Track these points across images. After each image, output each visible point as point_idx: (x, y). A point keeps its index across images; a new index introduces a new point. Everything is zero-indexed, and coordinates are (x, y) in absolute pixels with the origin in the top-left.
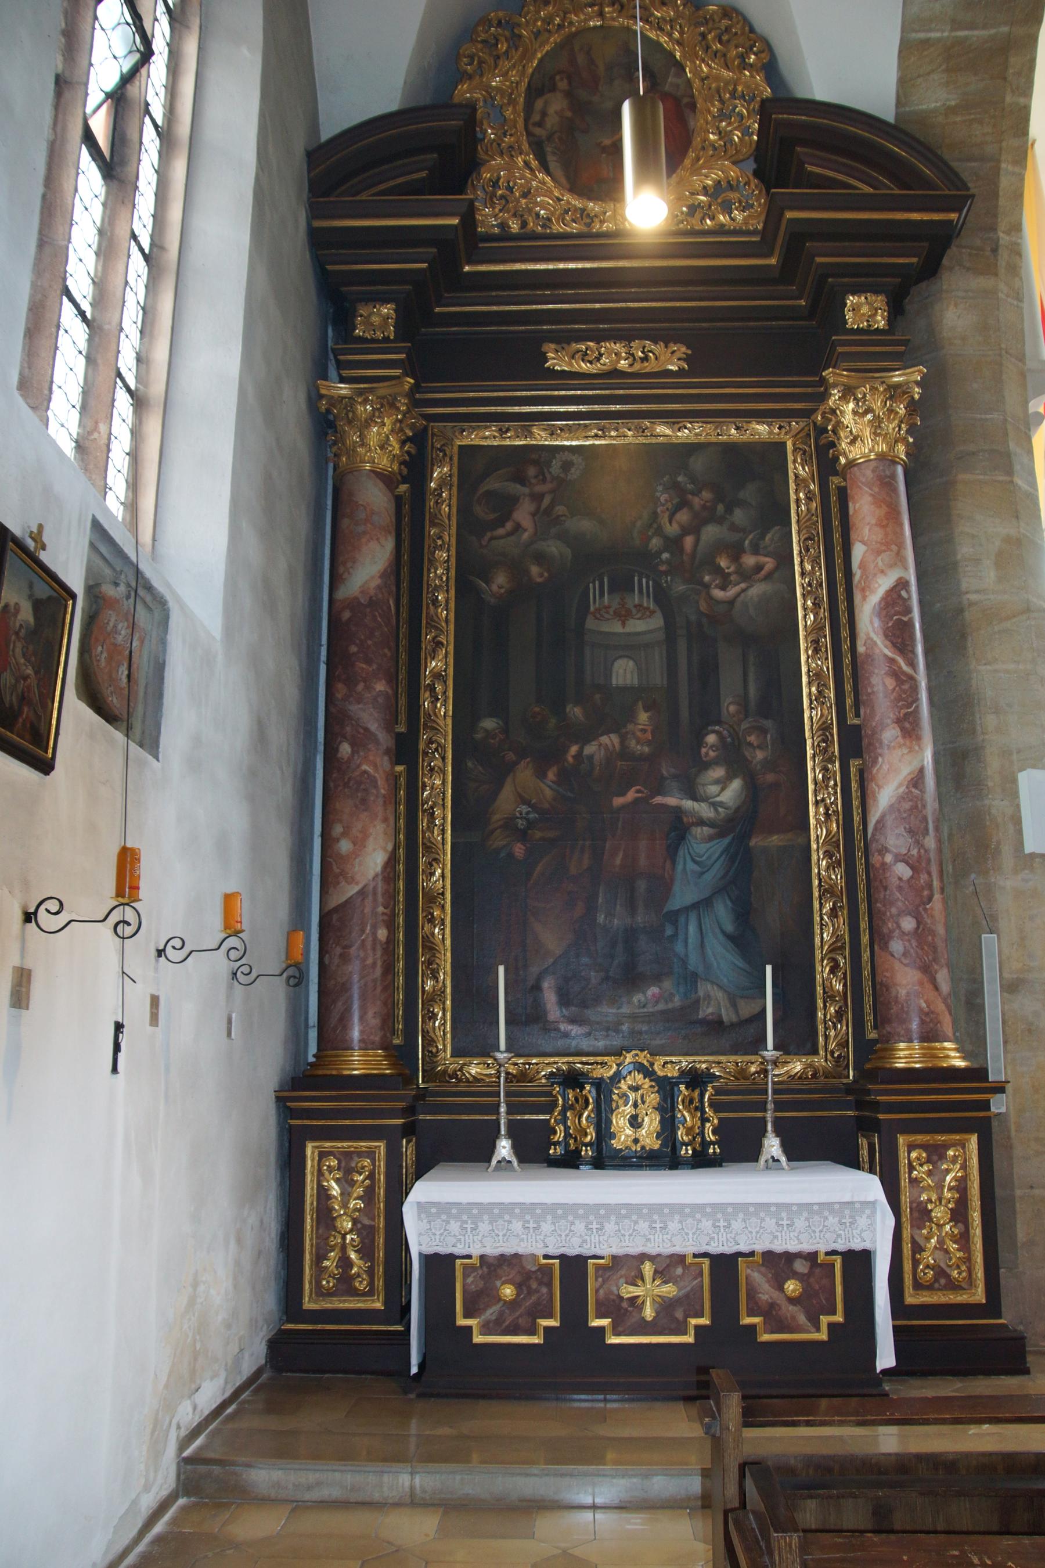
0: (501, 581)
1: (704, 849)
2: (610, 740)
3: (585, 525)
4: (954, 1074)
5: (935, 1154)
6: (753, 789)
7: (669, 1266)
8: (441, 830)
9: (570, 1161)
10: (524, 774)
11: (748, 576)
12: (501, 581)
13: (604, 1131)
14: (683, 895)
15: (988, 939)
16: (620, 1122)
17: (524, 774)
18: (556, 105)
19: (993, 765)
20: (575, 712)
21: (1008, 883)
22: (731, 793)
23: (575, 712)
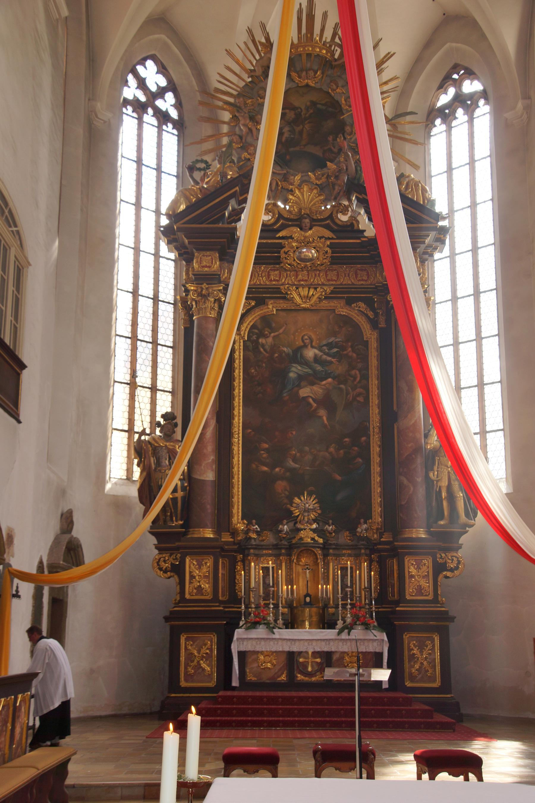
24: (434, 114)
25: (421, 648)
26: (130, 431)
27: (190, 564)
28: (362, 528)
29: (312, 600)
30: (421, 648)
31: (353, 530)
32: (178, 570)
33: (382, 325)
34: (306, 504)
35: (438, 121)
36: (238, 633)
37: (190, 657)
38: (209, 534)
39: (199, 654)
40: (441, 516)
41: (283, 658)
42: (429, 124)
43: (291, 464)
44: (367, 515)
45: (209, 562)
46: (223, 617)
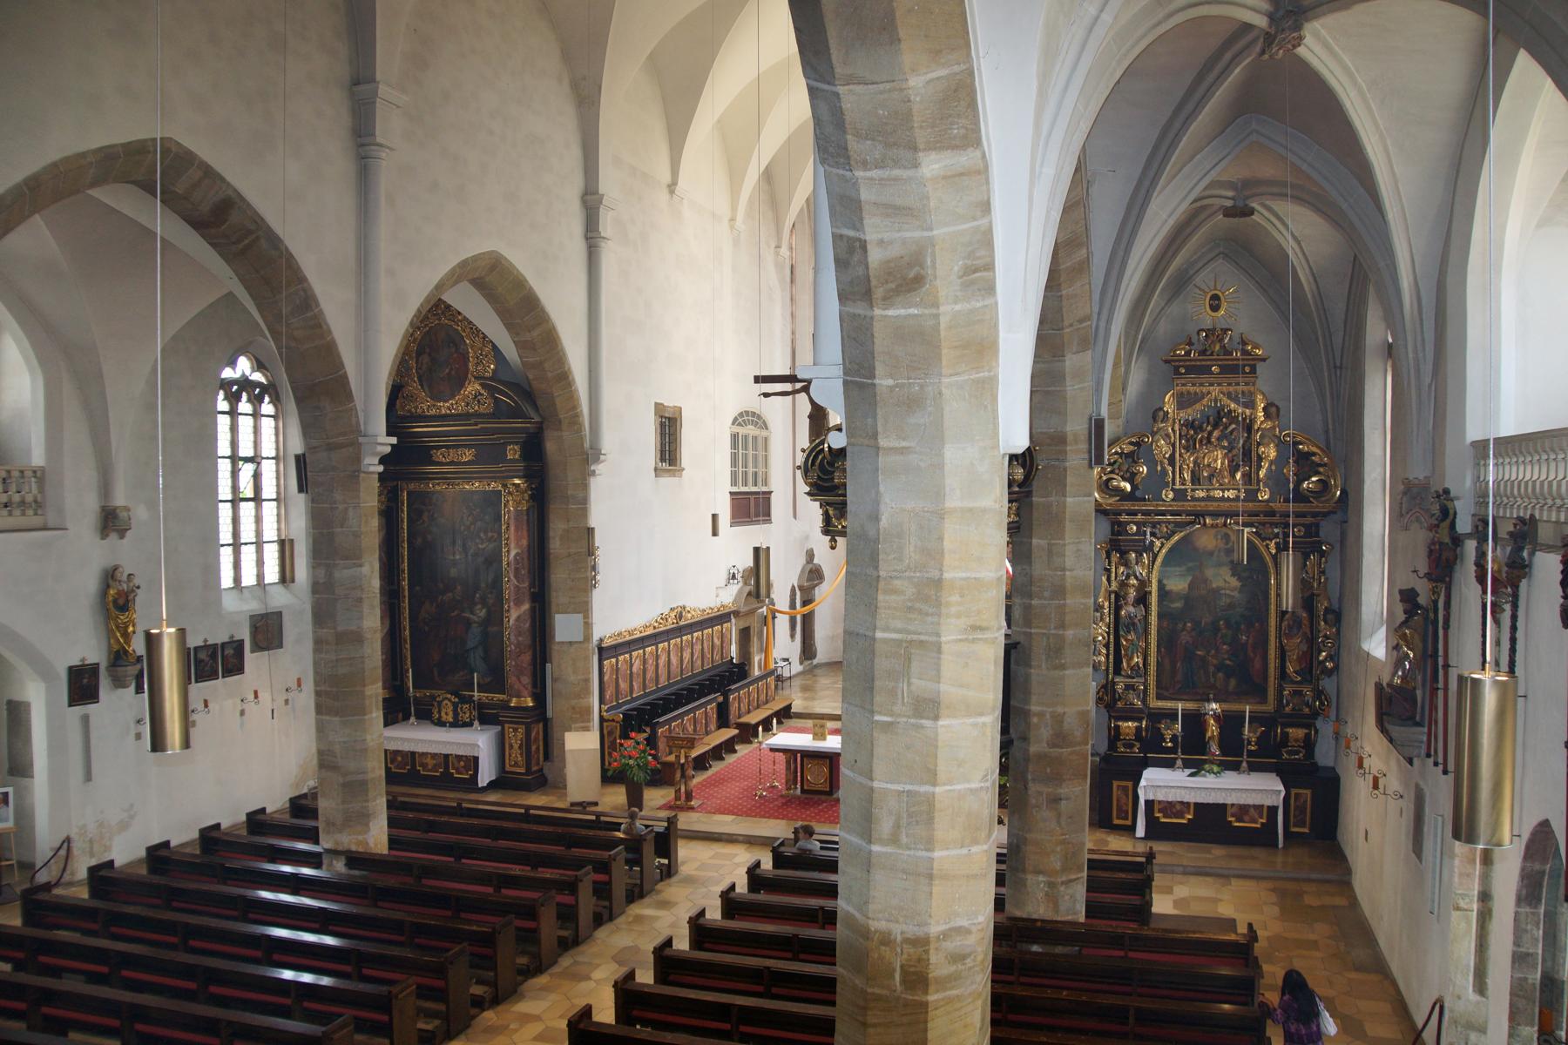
1: (476, 629)
4: (526, 709)
5: (515, 730)
6: (489, 613)
7: (434, 756)
8: (407, 623)
11: (490, 540)
14: (470, 644)
15: (548, 666)
18: (425, 359)
19: (554, 608)
21: (555, 647)
22: (483, 613)
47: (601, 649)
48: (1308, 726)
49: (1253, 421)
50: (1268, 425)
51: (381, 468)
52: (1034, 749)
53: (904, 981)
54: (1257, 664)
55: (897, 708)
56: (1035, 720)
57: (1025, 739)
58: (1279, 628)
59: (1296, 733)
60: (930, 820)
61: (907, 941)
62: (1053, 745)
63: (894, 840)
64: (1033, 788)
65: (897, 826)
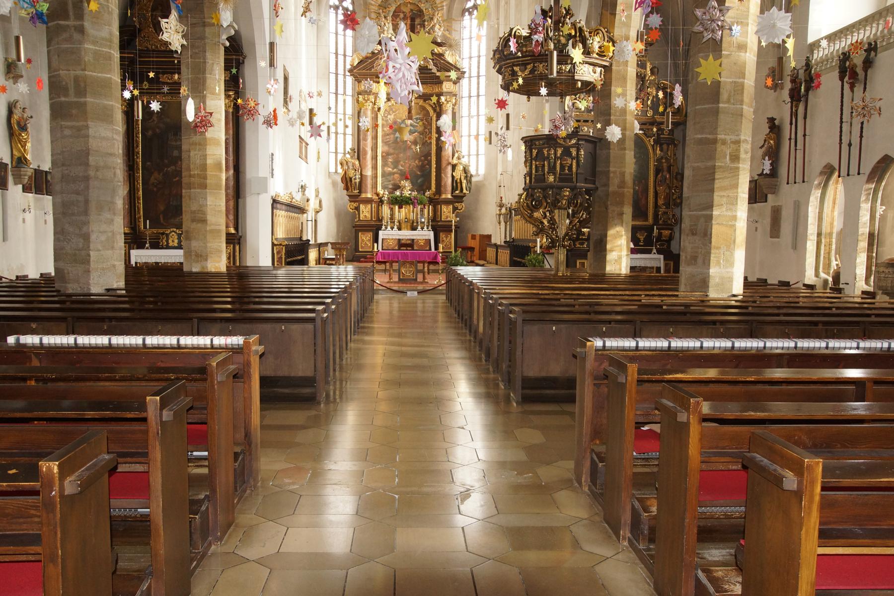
0: (150, 133)
2: (173, 167)
3: (168, 120)
9: (162, 248)
10: (156, 175)
12: (150, 133)
13: (168, 243)
16: (170, 241)
17: (156, 175)
20: (166, 161)
23: (166, 161)
24: (464, 11)
25: (447, 237)
26: (336, 153)
27: (362, 207)
28: (427, 193)
29: (407, 220)
30: (447, 237)
31: (424, 194)
32: (357, 209)
33: (438, 109)
34: (407, 184)
35: (467, 14)
36: (380, 232)
37: (363, 240)
38: (369, 196)
39: (365, 239)
40: (457, 189)
41: (396, 242)
42: (463, 15)
43: (400, 168)
44: (430, 188)
45: (369, 206)
46: (375, 228)
47: (275, 201)
48: (672, 229)
49: (645, 76)
50: (652, 78)
51: (228, 44)
52: (611, 189)
53: (730, 159)
54: (643, 201)
55: (731, 49)
56: (612, 175)
57: (607, 185)
58: (655, 182)
59: (666, 233)
60: (743, 93)
61: (732, 142)
62: (620, 187)
63: (728, 101)
64: (611, 208)
65: (730, 96)
